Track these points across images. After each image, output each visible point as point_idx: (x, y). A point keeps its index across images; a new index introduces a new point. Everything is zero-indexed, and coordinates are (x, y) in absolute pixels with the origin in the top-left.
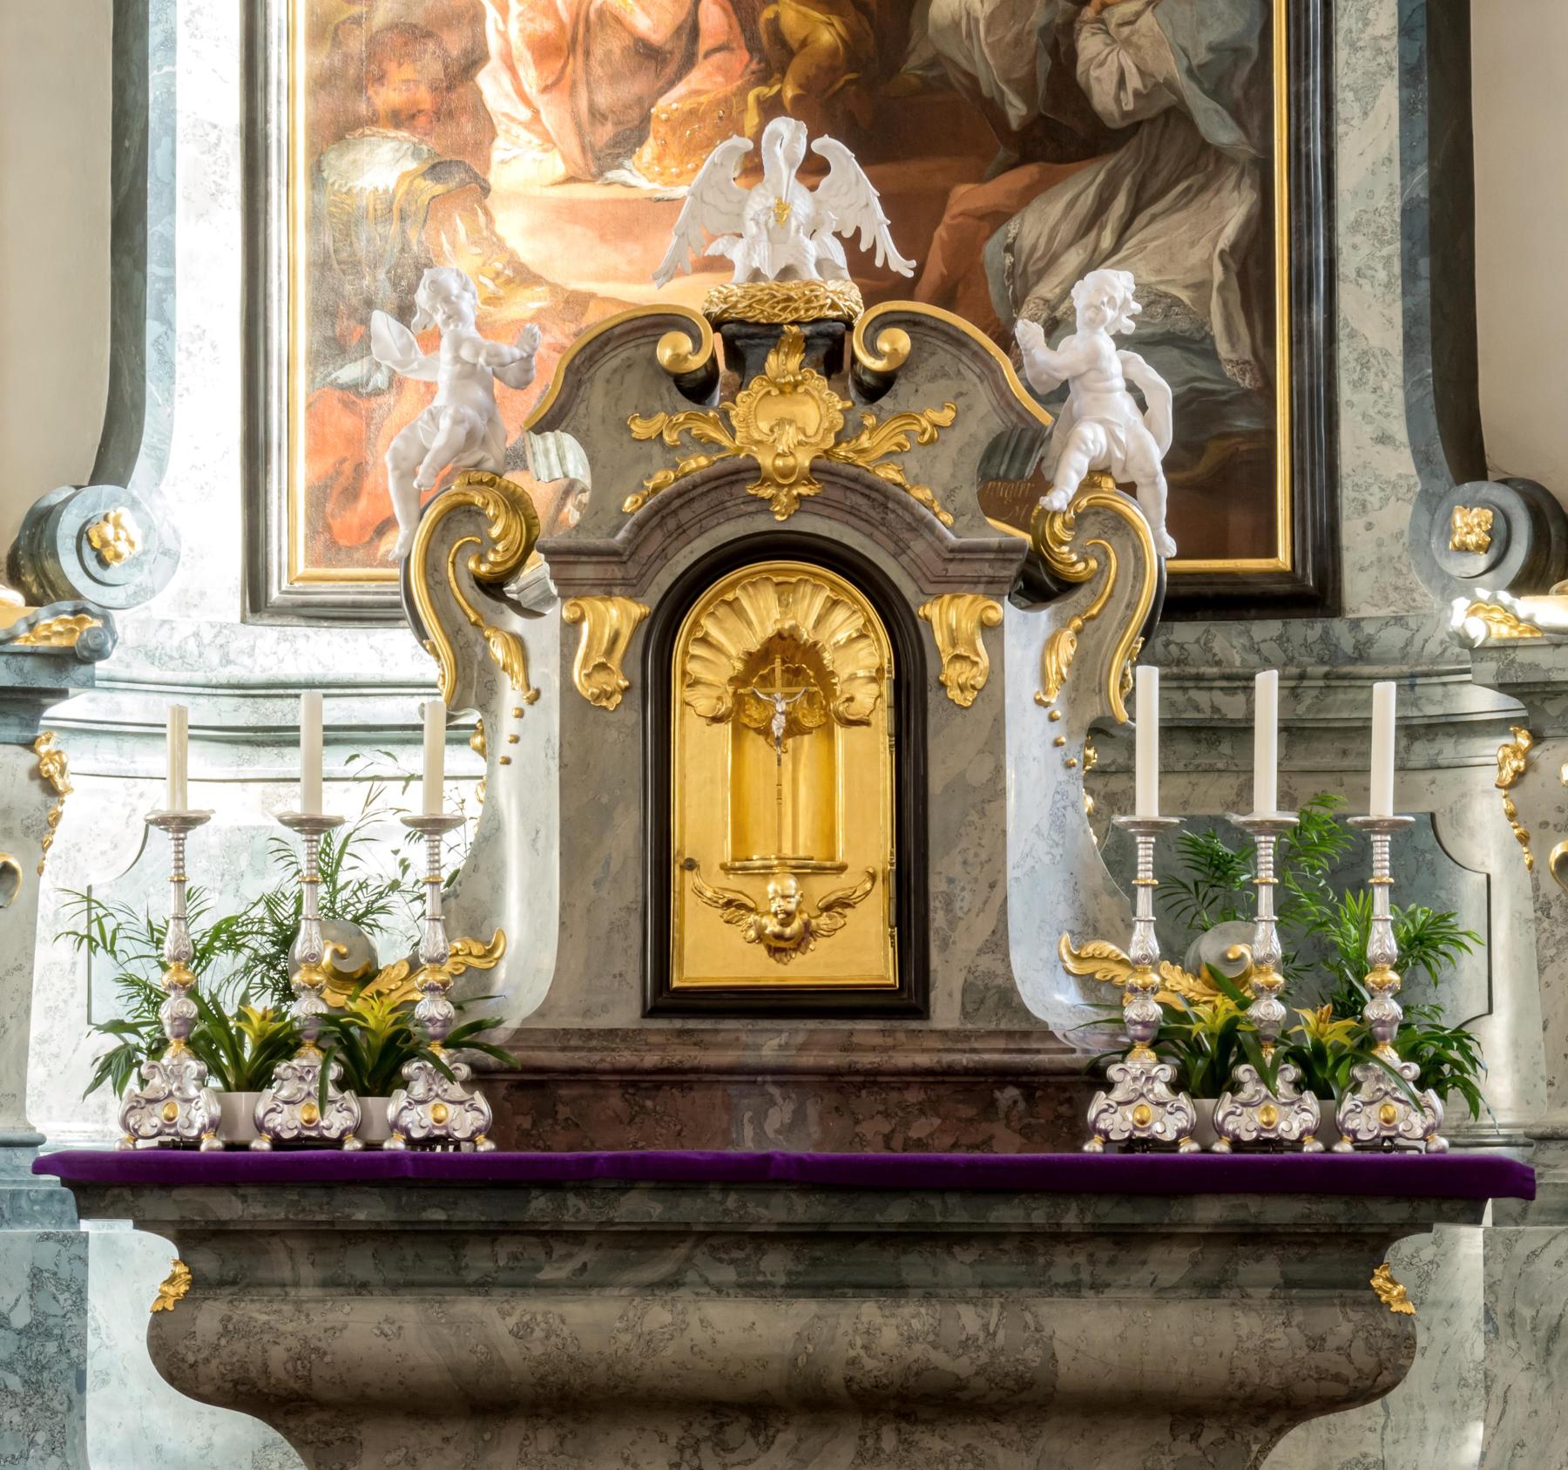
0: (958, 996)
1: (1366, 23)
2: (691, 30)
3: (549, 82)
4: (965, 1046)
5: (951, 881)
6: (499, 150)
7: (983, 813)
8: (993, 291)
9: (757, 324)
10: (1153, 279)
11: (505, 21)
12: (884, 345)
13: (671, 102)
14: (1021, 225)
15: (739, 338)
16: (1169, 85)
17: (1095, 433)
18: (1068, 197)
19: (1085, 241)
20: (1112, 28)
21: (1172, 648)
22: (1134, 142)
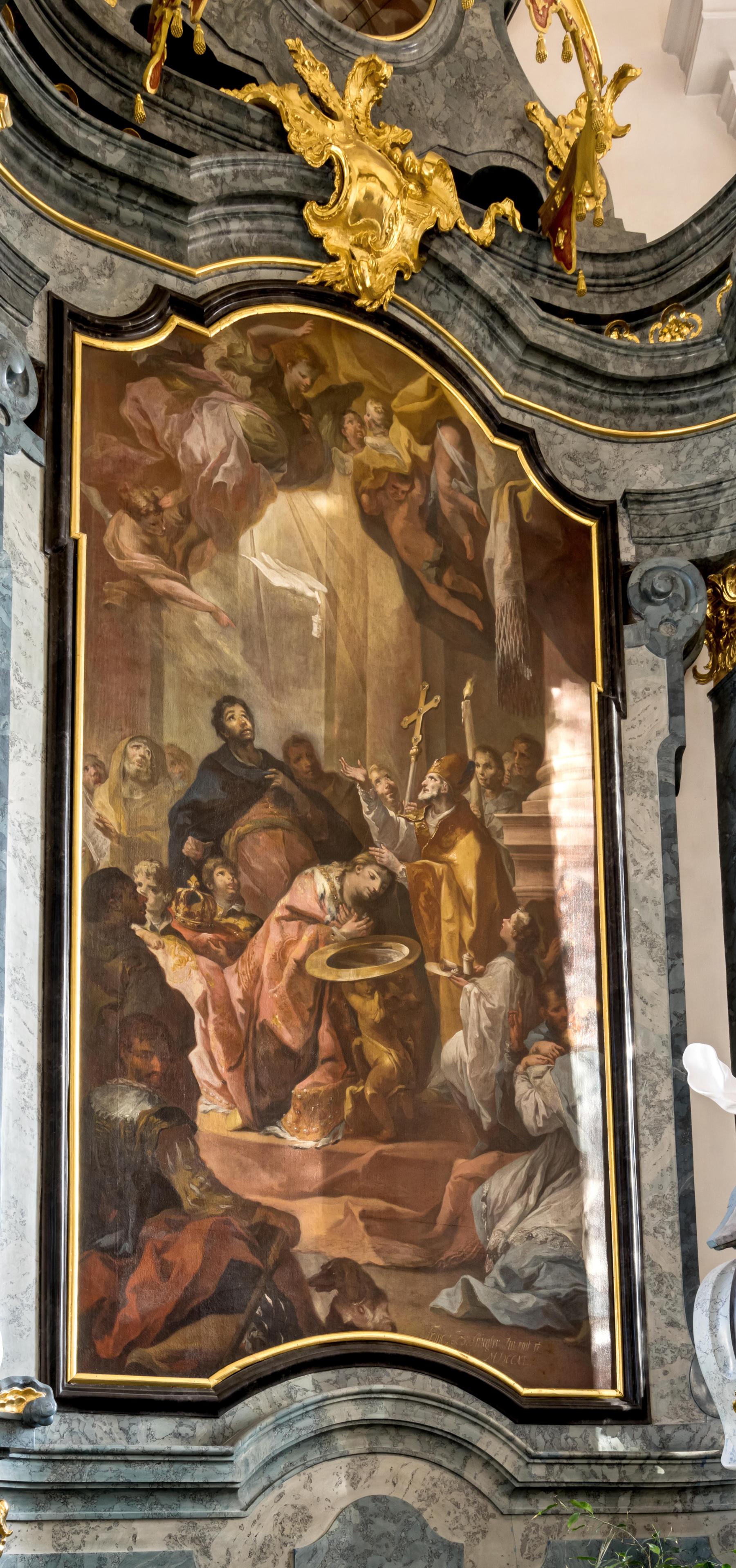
1: (655, 1093)
2: (313, 1043)
3: (233, 1064)
6: (203, 1106)
11: (206, 1023)
13: (302, 1088)
16: (559, 1114)
18: (512, 1173)
20: (531, 1078)
22: (543, 1145)
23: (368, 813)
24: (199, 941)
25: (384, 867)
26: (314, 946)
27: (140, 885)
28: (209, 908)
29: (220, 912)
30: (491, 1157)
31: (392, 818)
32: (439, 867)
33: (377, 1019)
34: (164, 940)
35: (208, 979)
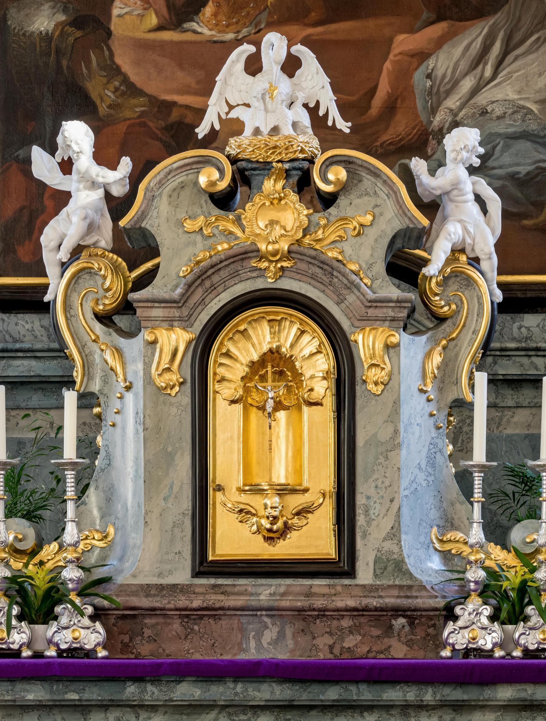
0: (371, 564)
4: (376, 594)
5: (368, 498)
7: (387, 458)
8: (419, 104)
9: (257, 162)
10: (516, 97)
12: (331, 177)
14: (437, 61)
15: (247, 170)
17: (456, 228)
18: (465, 43)
19: (475, 72)
21: (523, 330)
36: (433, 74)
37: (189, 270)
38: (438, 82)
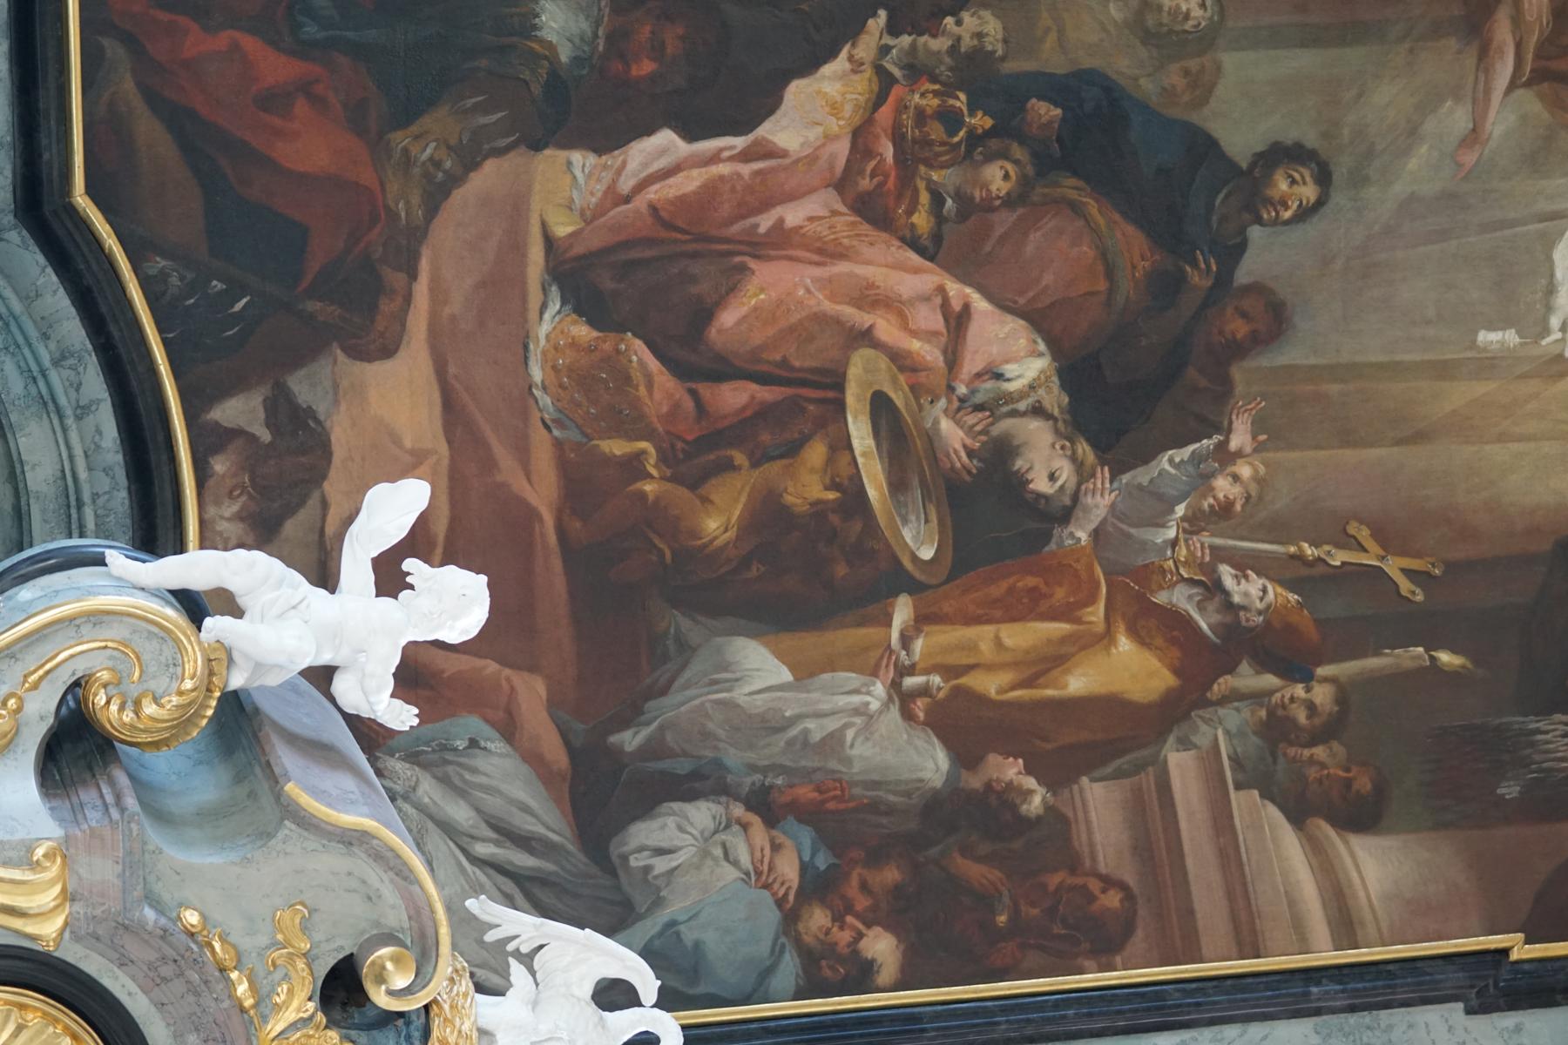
2: (724, 370)
3: (663, 214)
11: (731, 159)
13: (639, 352)
14: (501, 755)
16: (658, 903)
18: (533, 804)
19: (484, 825)
20: (722, 837)
22: (594, 870)
23: (1171, 461)
24: (877, 137)
25: (1076, 497)
26: (901, 361)
27: (959, 23)
28: (938, 155)
29: (935, 176)
30: (557, 755)
31: (1172, 511)
32: (1096, 614)
33: (789, 499)
34: (868, 72)
35: (812, 159)
36: (477, 751)
37: (193, 930)
38: (462, 760)
